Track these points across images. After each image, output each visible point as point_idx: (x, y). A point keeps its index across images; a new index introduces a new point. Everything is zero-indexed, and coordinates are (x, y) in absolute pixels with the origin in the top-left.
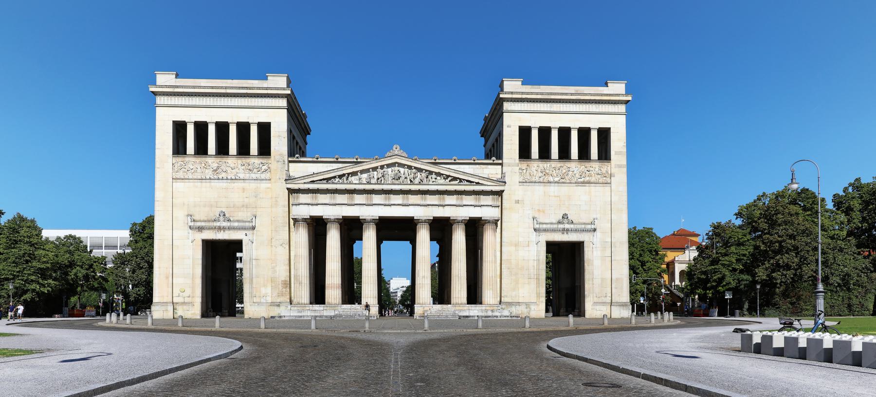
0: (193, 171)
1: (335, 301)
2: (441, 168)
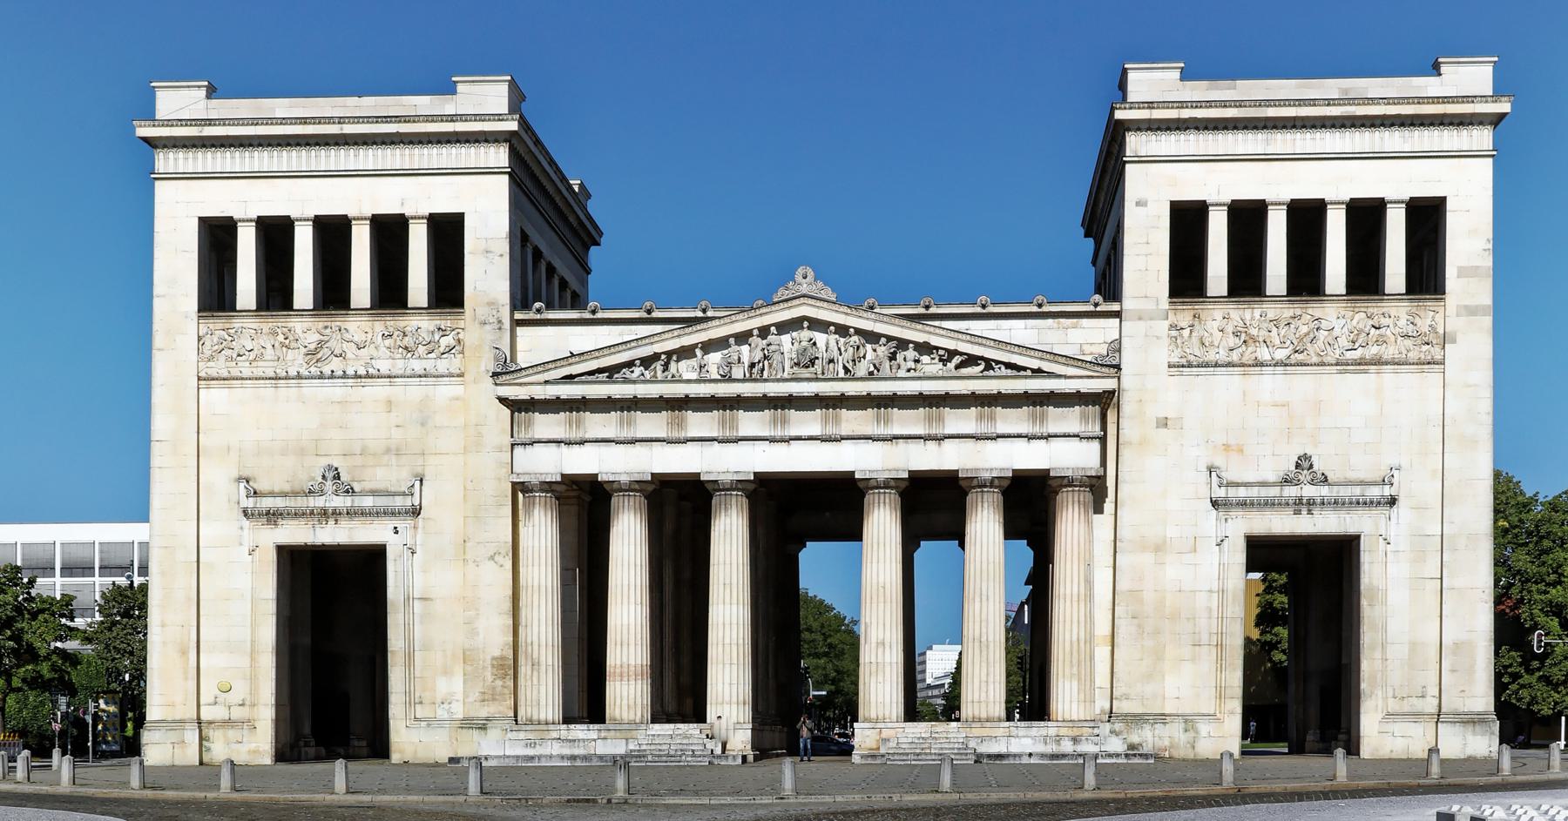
1: (632, 713)
2: (932, 329)
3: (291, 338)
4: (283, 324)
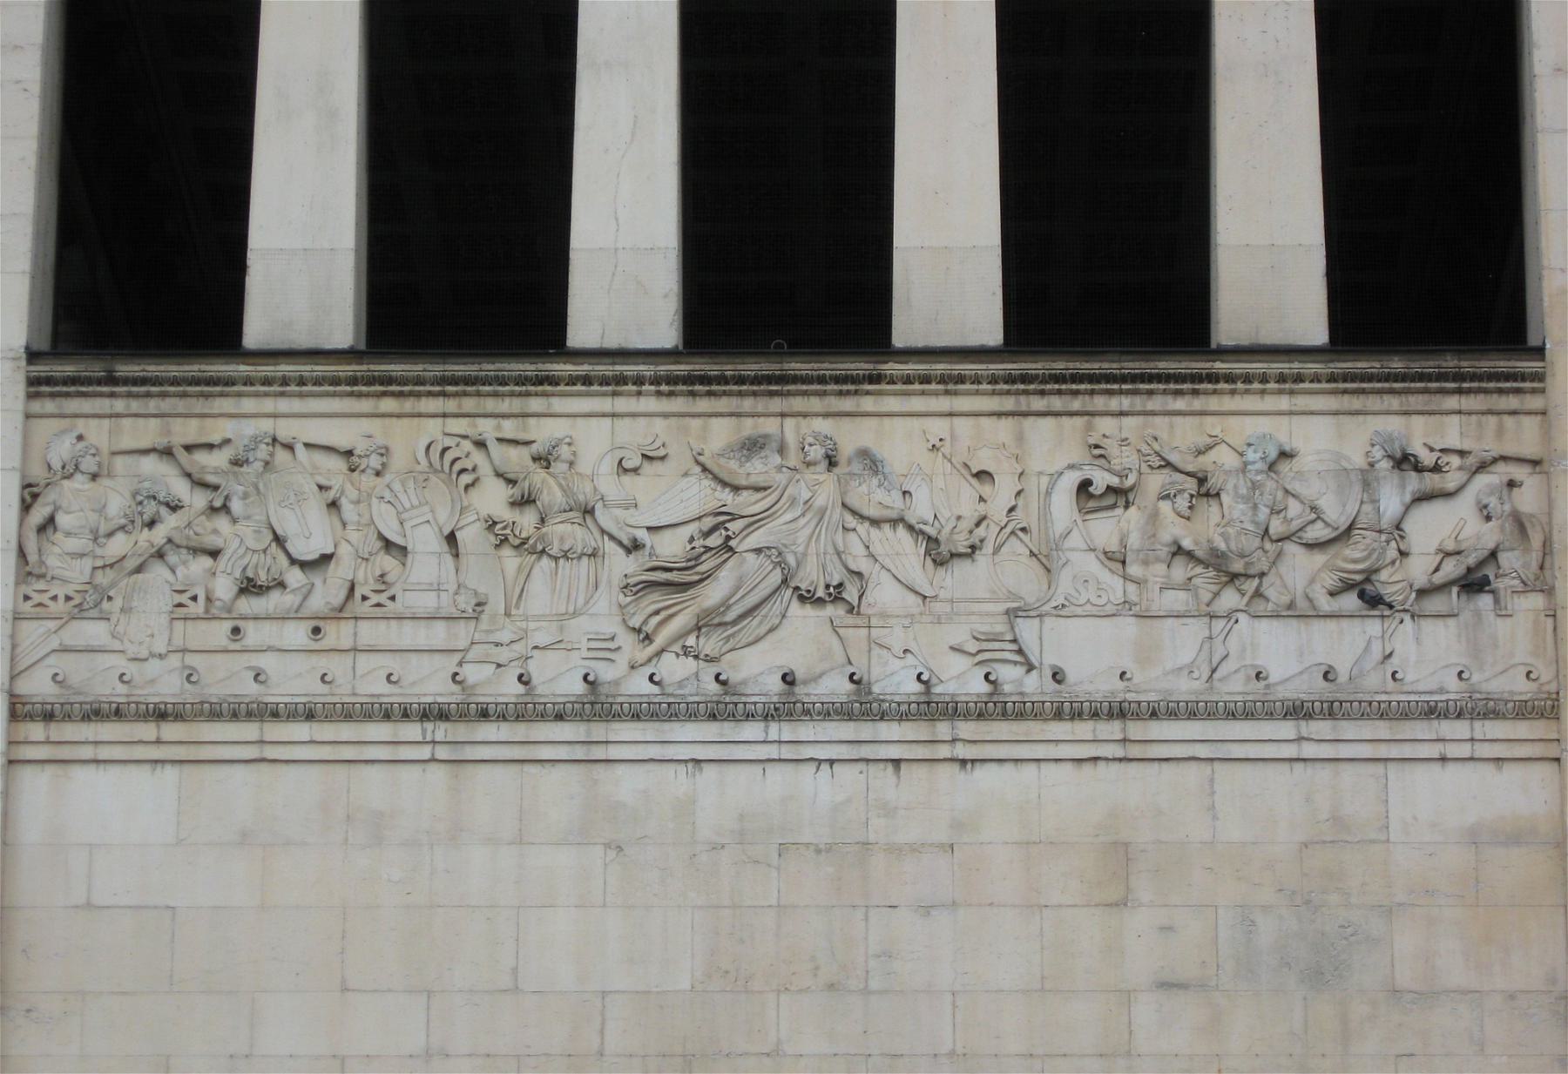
0: (327, 592)
3: (551, 493)
4: (509, 428)
